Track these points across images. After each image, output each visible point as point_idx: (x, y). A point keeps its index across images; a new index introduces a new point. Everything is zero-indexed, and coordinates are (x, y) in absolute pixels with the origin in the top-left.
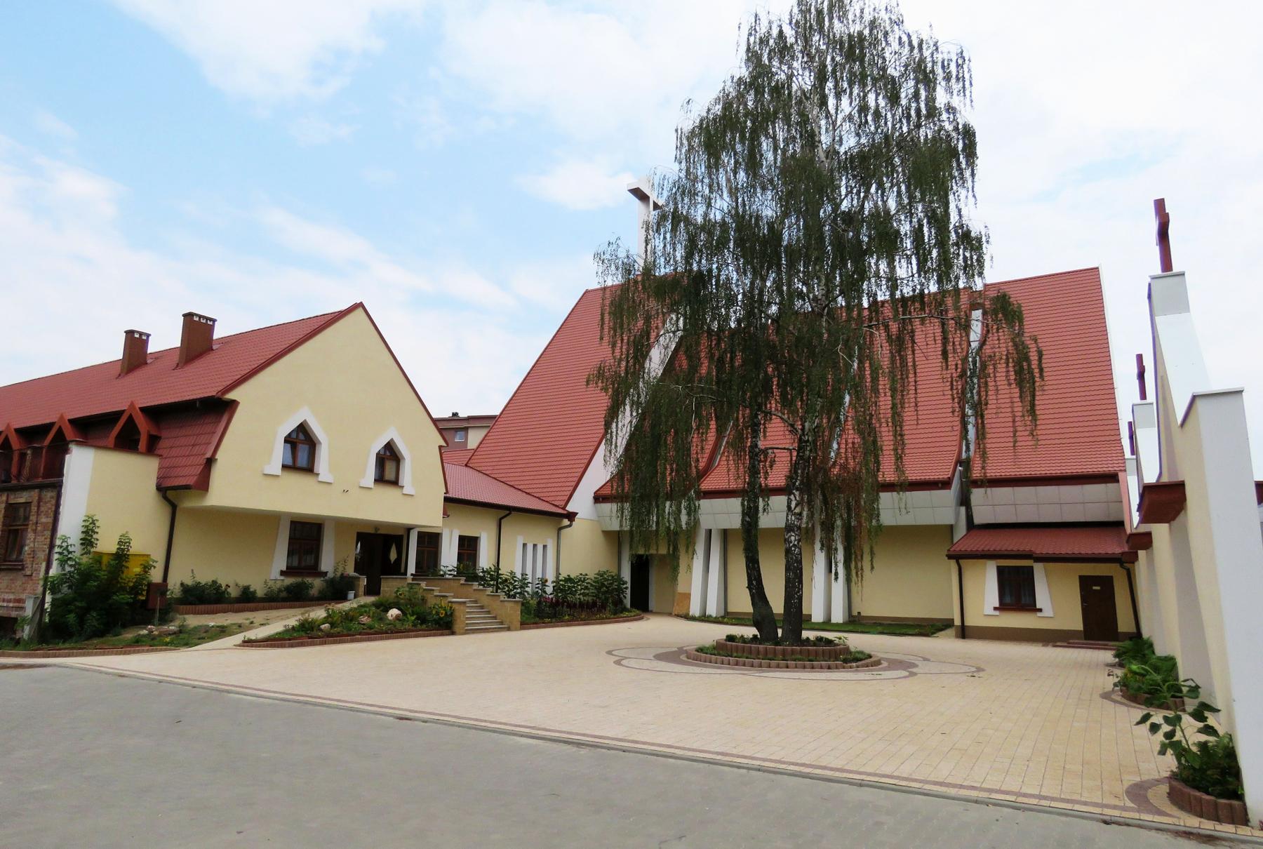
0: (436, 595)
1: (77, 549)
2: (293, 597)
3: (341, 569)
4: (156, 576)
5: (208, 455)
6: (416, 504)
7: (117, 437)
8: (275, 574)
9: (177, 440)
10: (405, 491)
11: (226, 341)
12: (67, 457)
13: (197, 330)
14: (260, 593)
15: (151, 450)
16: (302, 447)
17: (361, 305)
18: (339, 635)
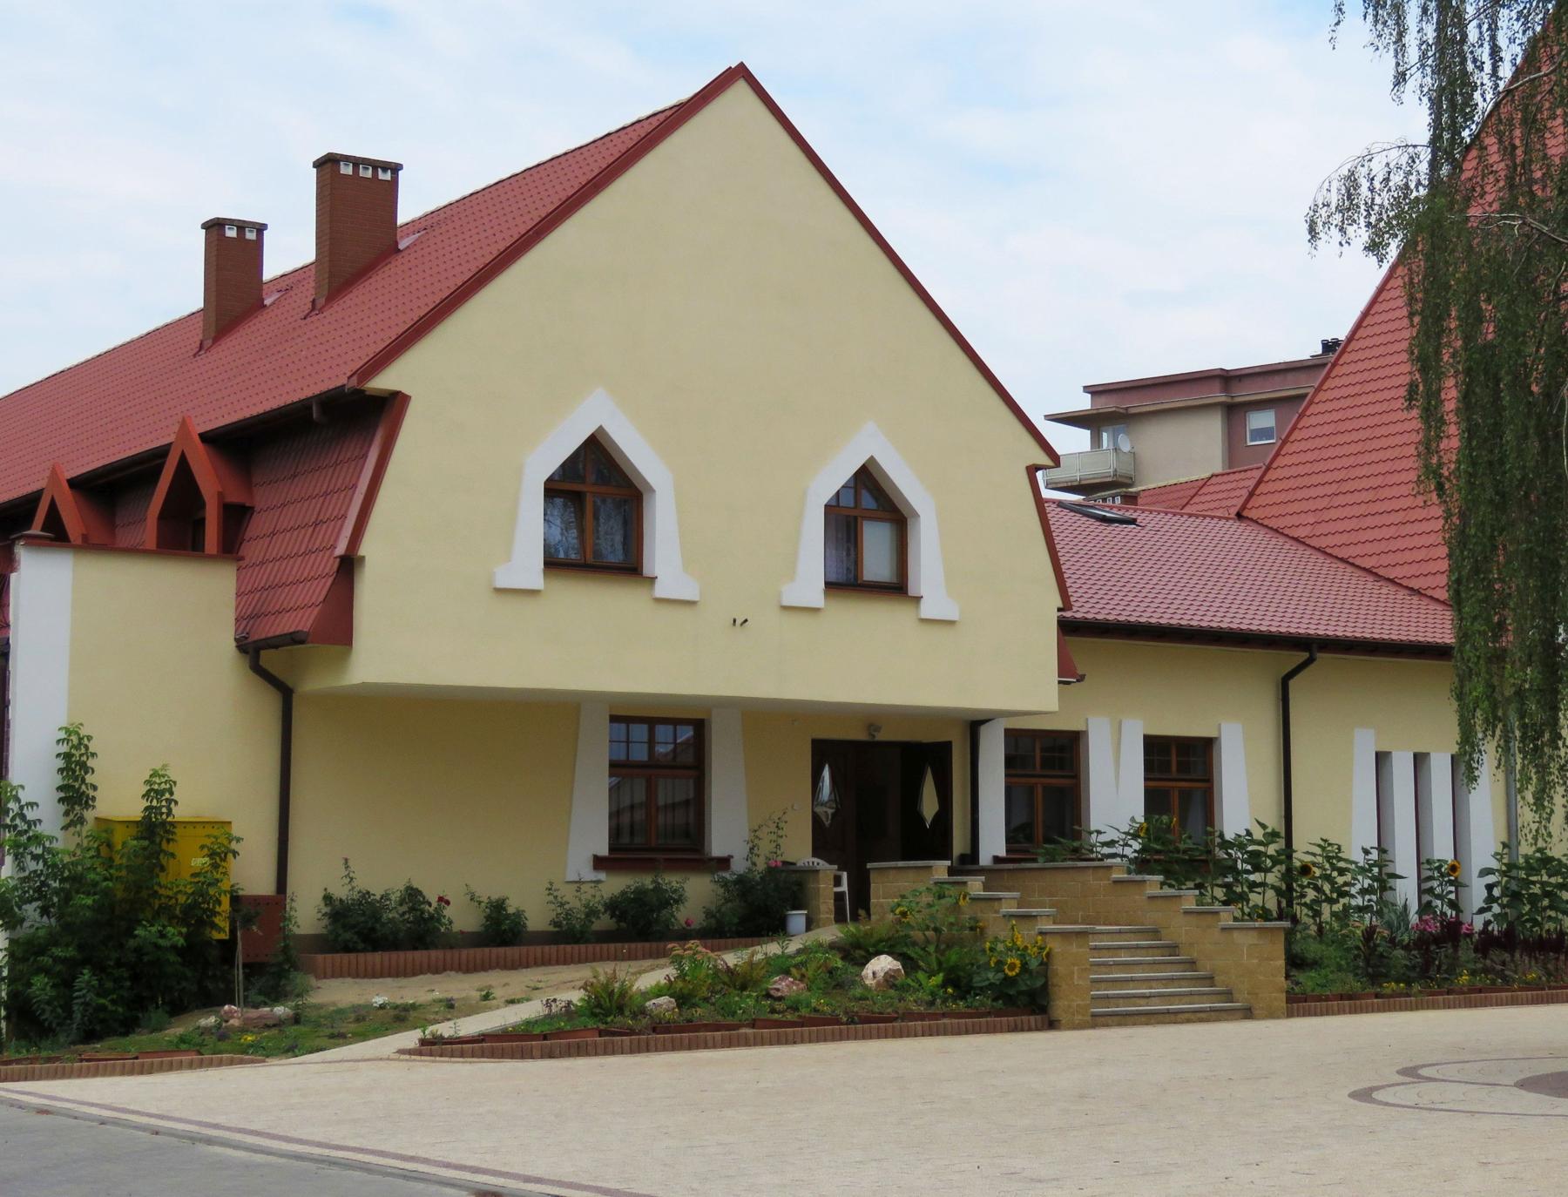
0: (1017, 920)
1: (48, 816)
2: (639, 925)
3: (765, 847)
4: (252, 873)
5: (341, 549)
6: (971, 644)
7: (163, 516)
8: (578, 865)
9: (284, 504)
10: (928, 609)
11: (431, 223)
12: (13, 576)
13: (354, 195)
14: (537, 918)
15: (230, 548)
16: (598, 511)
17: (740, 73)
18: (690, 1026)
